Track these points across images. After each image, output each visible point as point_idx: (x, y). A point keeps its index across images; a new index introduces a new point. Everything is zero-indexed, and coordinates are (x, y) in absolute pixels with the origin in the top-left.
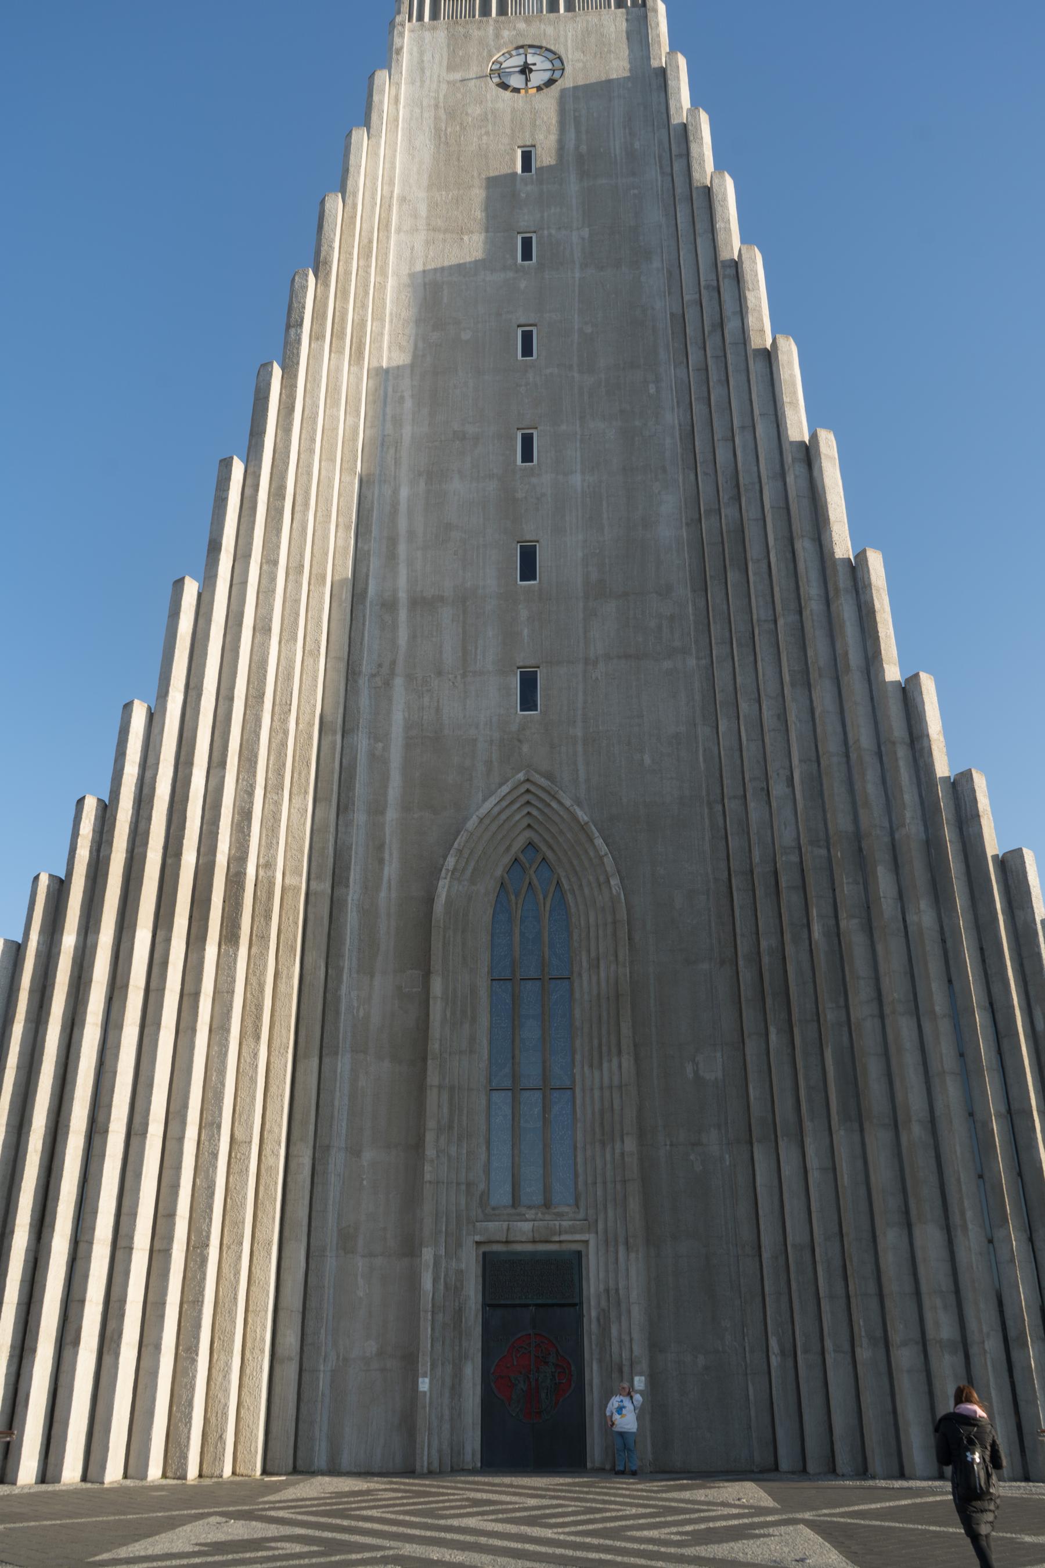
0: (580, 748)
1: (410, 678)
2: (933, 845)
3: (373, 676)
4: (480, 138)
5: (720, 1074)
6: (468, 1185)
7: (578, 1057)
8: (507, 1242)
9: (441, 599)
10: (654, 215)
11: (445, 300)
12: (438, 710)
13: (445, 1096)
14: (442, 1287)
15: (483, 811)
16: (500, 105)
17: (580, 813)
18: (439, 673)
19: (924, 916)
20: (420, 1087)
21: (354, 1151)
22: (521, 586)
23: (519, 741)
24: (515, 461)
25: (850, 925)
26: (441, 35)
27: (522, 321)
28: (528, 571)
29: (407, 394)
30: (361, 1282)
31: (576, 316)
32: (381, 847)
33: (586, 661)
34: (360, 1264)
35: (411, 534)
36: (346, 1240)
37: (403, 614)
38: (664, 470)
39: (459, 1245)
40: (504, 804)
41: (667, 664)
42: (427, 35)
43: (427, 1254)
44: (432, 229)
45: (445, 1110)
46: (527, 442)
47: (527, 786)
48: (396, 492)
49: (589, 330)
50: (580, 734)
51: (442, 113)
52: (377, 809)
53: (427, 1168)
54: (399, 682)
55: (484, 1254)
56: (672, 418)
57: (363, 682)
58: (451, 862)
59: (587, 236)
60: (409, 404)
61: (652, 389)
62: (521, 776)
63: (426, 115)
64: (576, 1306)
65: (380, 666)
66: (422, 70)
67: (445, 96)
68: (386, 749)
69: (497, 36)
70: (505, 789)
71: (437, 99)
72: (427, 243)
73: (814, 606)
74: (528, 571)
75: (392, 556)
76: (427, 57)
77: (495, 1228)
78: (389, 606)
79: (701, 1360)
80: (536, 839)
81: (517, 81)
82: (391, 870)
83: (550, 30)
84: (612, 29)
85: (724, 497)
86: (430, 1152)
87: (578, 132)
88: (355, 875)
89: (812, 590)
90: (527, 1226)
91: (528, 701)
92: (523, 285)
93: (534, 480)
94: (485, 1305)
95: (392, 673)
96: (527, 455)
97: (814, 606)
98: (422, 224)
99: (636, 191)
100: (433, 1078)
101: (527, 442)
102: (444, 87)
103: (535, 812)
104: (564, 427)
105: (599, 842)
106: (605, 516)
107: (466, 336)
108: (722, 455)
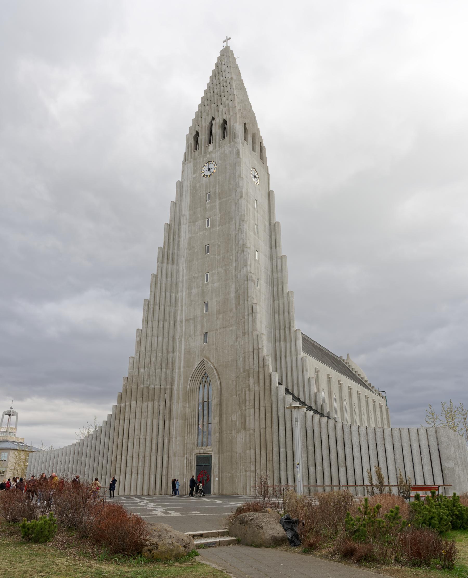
0: (214, 350)
1: (185, 338)
3: (179, 339)
4: (199, 193)
5: (235, 419)
6: (193, 443)
9: (190, 319)
11: (192, 242)
14: (188, 462)
16: (203, 182)
19: (256, 388)
21: (176, 438)
23: (204, 350)
24: (204, 282)
26: (192, 164)
27: (207, 244)
29: (185, 268)
30: (177, 462)
31: (217, 240)
32: (180, 376)
33: (216, 329)
34: (177, 458)
35: (185, 303)
38: (233, 279)
40: (199, 365)
41: (231, 328)
43: (185, 456)
44: (190, 222)
45: (189, 429)
47: (203, 361)
49: (219, 244)
50: (214, 347)
51: (192, 187)
52: (179, 368)
53: (186, 441)
54: (183, 339)
55: (196, 456)
59: (220, 216)
60: (185, 271)
61: (231, 258)
62: (202, 359)
63: (189, 189)
64: (211, 465)
65: (180, 336)
66: (188, 175)
68: (181, 355)
69: (203, 160)
71: (191, 183)
72: (189, 226)
75: (182, 310)
76: (189, 170)
77: (197, 451)
78: (181, 322)
79: (229, 475)
81: (207, 173)
82: (182, 381)
84: (227, 151)
88: (176, 383)
93: (208, 286)
94: (196, 465)
95: (182, 337)
98: (188, 220)
99: (230, 201)
100: (187, 424)
102: (192, 179)
103: (205, 366)
104: (214, 271)
106: (221, 293)
107: (196, 251)
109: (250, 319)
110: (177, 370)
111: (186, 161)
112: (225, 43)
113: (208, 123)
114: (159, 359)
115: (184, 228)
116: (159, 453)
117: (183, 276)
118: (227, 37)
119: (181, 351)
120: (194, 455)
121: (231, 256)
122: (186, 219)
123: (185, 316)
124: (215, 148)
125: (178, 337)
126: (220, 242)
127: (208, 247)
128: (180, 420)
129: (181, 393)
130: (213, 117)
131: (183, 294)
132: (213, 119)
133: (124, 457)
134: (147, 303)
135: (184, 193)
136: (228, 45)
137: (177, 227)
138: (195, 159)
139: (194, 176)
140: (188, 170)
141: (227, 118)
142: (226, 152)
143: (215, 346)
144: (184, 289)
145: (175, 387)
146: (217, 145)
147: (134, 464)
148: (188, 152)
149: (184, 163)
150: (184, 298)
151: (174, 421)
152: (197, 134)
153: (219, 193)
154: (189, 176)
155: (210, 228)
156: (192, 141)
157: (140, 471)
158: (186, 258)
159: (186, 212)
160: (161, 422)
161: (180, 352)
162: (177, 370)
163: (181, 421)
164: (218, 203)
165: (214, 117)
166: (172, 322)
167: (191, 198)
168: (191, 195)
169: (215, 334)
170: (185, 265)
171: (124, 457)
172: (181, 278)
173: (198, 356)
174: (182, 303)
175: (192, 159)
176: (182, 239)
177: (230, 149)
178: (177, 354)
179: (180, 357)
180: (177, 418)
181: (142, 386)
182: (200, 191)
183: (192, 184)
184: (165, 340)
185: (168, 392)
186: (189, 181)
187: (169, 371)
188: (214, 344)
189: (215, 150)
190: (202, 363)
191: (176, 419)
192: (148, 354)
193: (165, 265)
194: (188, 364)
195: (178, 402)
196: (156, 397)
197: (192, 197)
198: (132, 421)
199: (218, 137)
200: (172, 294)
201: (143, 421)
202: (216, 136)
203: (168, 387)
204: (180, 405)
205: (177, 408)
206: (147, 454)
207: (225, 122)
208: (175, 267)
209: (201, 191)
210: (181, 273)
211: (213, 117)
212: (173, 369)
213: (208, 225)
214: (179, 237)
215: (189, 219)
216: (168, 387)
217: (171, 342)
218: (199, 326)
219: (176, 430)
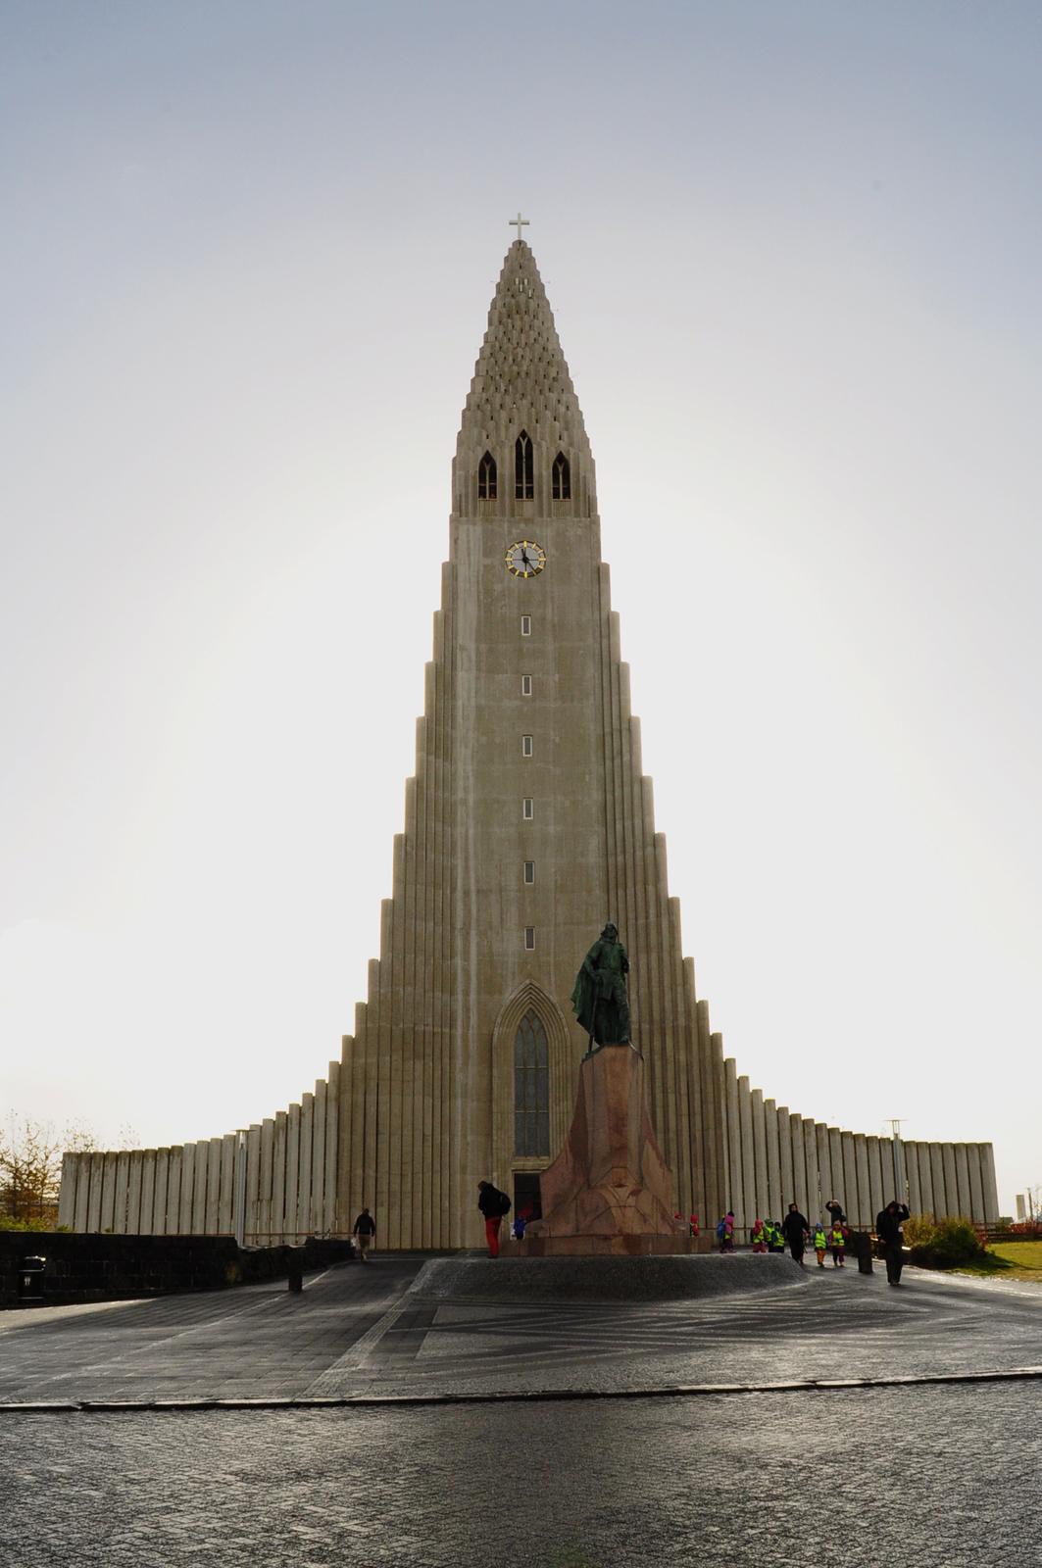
0: (552, 968)
2: (688, 1029)
7: (550, 1100)
10: (591, 671)
12: (490, 947)
13: (499, 1115)
15: (512, 997)
17: (551, 997)
18: (491, 928)
20: (491, 1112)
21: (464, 1136)
22: (529, 886)
25: (656, 1057)
26: (479, 529)
28: (529, 879)
29: (470, 774)
36: (464, 1169)
37: (473, 897)
39: (505, 1172)
41: (590, 928)
42: (471, 527)
43: (495, 1174)
44: (479, 669)
48: (467, 831)
50: (552, 961)
51: (481, 586)
52: (466, 993)
53: (494, 1144)
54: (473, 933)
56: (596, 796)
57: (457, 933)
58: (499, 1020)
59: (557, 679)
60: (471, 780)
61: (587, 780)
62: (528, 982)
63: (473, 589)
65: (464, 924)
66: (469, 555)
67: (483, 575)
68: (469, 964)
69: (510, 532)
70: (522, 987)
71: (478, 577)
72: (478, 678)
73: (652, 918)
75: (466, 869)
76: (472, 545)
78: (466, 893)
81: (520, 567)
82: (474, 1020)
83: (538, 532)
85: (619, 850)
86: (495, 1138)
87: (553, 609)
88: (459, 1023)
89: (652, 911)
90: (531, 1163)
92: (526, 709)
94: (515, 1193)
97: (652, 918)
98: (474, 663)
100: (495, 1110)
102: (482, 568)
105: (560, 1012)
107: (497, 740)
108: (619, 827)
110: (460, 997)
111: (461, 516)
113: (513, 443)
114: (430, 968)
116: (437, 1167)
117: (466, 790)
118: (519, 215)
119: (469, 958)
120: (510, 1173)
121: (587, 777)
122: (470, 661)
123: (477, 881)
124: (541, 515)
125: (459, 925)
126: (561, 738)
127: (528, 741)
128: (473, 1101)
129: (473, 1047)
131: (466, 828)
132: (523, 434)
133: (371, 1173)
134: (404, 842)
135: (461, 595)
136: (522, 239)
137: (448, 672)
138: (487, 520)
139: (488, 561)
140: (468, 542)
141: (569, 451)
142: (567, 534)
143: (555, 957)
144: (471, 822)
145: (459, 1031)
146: (545, 507)
147: (396, 1187)
148: (467, 496)
149: (455, 521)
151: (459, 1102)
152: (488, 459)
153: (554, 626)
154: (472, 558)
155: (533, 699)
156: (474, 469)
157: (408, 1202)
158: (473, 752)
159: (466, 638)
160: (438, 1103)
161: (466, 958)
162: (460, 997)
163: (475, 1103)
164: (550, 647)
166: (449, 892)
167: (479, 611)
168: (479, 606)
169: (553, 934)
171: (371, 1173)
172: (460, 794)
173: (514, 973)
174: (466, 850)
175: (479, 518)
176: (460, 703)
177: (579, 532)
178: (459, 961)
179: (466, 972)
180: (465, 1095)
181: (401, 1026)
182: (503, 603)
183: (480, 579)
184: (439, 930)
185: (447, 1040)
186: (472, 569)
187: (447, 997)
188: (552, 951)
189: (538, 519)
190: (532, 991)
191: (462, 1097)
192: (410, 957)
193: (432, 758)
194: (490, 985)
195: (466, 1064)
196: (429, 1051)
197: (482, 613)
198: (384, 1098)
199: (545, 488)
200: (446, 828)
201: (408, 1099)
202: (540, 487)
203: (447, 1030)
204: (473, 1070)
205: (467, 1075)
206: (418, 1167)
207: (561, 459)
208: (447, 764)
209: (505, 605)
210: (460, 783)
211: (524, 431)
212: (452, 993)
213: (527, 691)
214: (454, 697)
215: (476, 662)
216: (447, 1030)
217: (448, 935)
218: (513, 910)
219: (464, 1122)
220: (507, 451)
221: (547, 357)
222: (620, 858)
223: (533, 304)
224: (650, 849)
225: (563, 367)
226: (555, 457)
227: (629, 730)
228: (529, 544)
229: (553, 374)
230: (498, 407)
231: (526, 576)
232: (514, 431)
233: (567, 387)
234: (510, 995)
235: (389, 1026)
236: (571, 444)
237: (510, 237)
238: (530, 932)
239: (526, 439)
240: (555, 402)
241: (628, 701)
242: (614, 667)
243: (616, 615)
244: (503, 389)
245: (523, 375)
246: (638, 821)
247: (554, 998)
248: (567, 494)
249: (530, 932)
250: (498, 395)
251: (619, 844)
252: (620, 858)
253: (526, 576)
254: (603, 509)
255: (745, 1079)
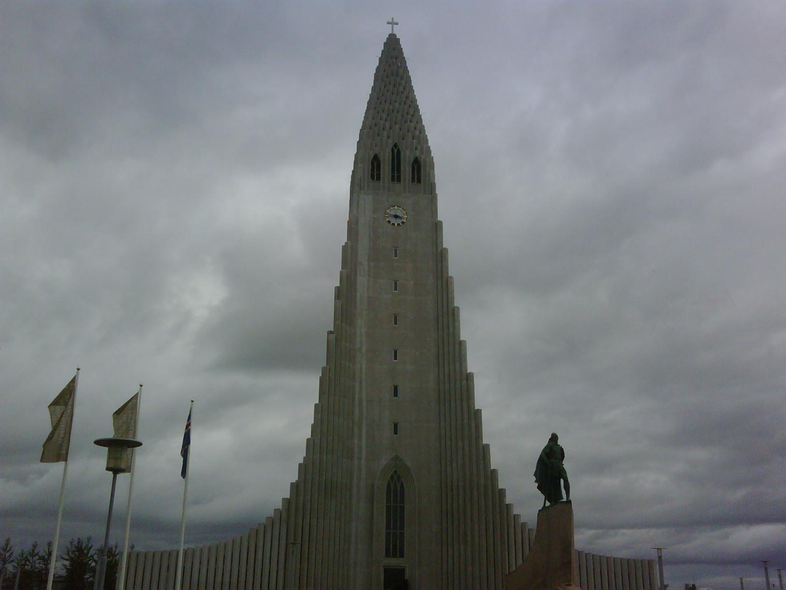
8: (390, 566)
28: (396, 395)
37: (365, 404)
46: (396, 352)
52: (360, 459)
54: (364, 424)
60: (364, 338)
73: (466, 421)
74: (396, 395)
78: (360, 403)
80: (397, 470)
81: (393, 220)
89: (466, 417)
91: (396, 432)
96: (396, 358)
97: (466, 421)
101: (396, 352)
108: (447, 370)
109: (473, 425)
110: (356, 462)
111: (361, 190)
112: (391, 25)
115: (362, 281)
118: (393, 19)
130: (396, 144)
132: (395, 146)
136: (394, 32)
145: (355, 481)
150: (364, 371)
152: (376, 158)
165: (398, 144)
170: (363, 330)
172: (358, 346)
176: (358, 294)
178: (356, 442)
179: (360, 447)
190: (396, 458)
193: (344, 324)
199: (407, 177)
211: (396, 144)
220: (387, 154)
221: (409, 103)
222: (447, 386)
223: (401, 71)
224: (464, 382)
225: (417, 109)
226: (413, 159)
227: (454, 315)
228: (399, 208)
229: (412, 113)
230: (382, 129)
231: (396, 225)
232: (391, 143)
233: (420, 120)
234: (384, 461)
235: (317, 479)
236: (422, 153)
237: (387, 30)
238: (396, 426)
239: (397, 148)
240: (413, 128)
241: (453, 298)
242: (444, 279)
243: (446, 250)
244: (384, 118)
245: (396, 111)
246: (457, 365)
247: (409, 464)
248: (419, 181)
249: (396, 426)
250: (382, 122)
251: (446, 378)
252: (447, 386)
253: (396, 225)
254: (438, 191)
255: (518, 516)
